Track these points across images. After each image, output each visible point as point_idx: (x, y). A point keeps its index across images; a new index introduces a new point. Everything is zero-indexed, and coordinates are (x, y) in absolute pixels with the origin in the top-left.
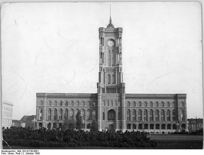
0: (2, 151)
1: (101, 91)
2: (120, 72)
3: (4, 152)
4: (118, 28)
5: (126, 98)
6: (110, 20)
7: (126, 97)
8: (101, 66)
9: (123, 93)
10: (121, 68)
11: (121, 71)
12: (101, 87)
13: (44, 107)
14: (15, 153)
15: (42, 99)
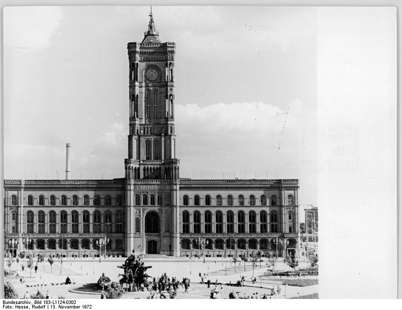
0: (4, 302)
1: (132, 174)
2: (171, 135)
3: (7, 305)
4: (165, 44)
5: (181, 188)
6: (152, 21)
7: (181, 186)
8: (132, 122)
9: (175, 178)
10: (171, 127)
11: (171, 132)
12: (132, 167)
13: (19, 209)
14: (30, 306)
15: (15, 193)
